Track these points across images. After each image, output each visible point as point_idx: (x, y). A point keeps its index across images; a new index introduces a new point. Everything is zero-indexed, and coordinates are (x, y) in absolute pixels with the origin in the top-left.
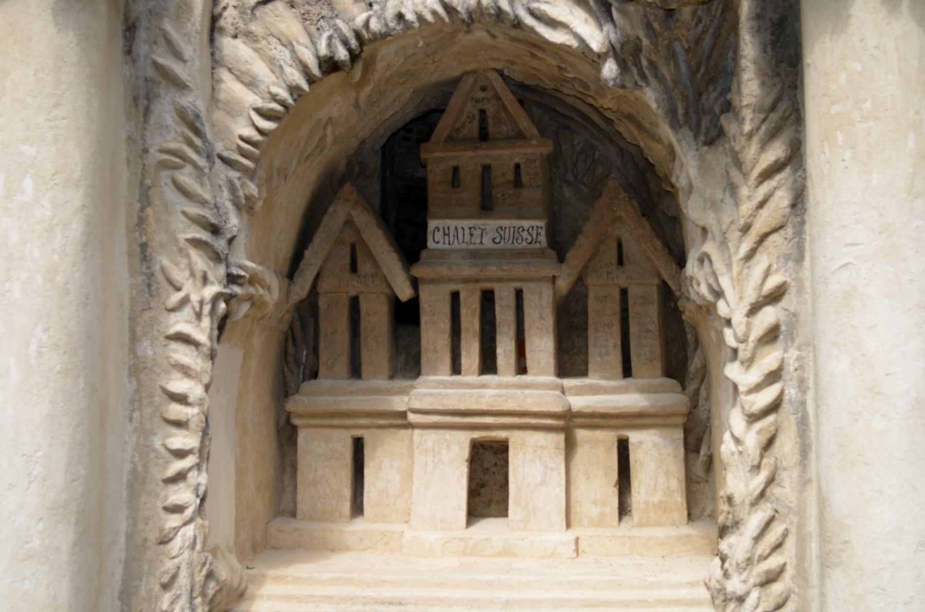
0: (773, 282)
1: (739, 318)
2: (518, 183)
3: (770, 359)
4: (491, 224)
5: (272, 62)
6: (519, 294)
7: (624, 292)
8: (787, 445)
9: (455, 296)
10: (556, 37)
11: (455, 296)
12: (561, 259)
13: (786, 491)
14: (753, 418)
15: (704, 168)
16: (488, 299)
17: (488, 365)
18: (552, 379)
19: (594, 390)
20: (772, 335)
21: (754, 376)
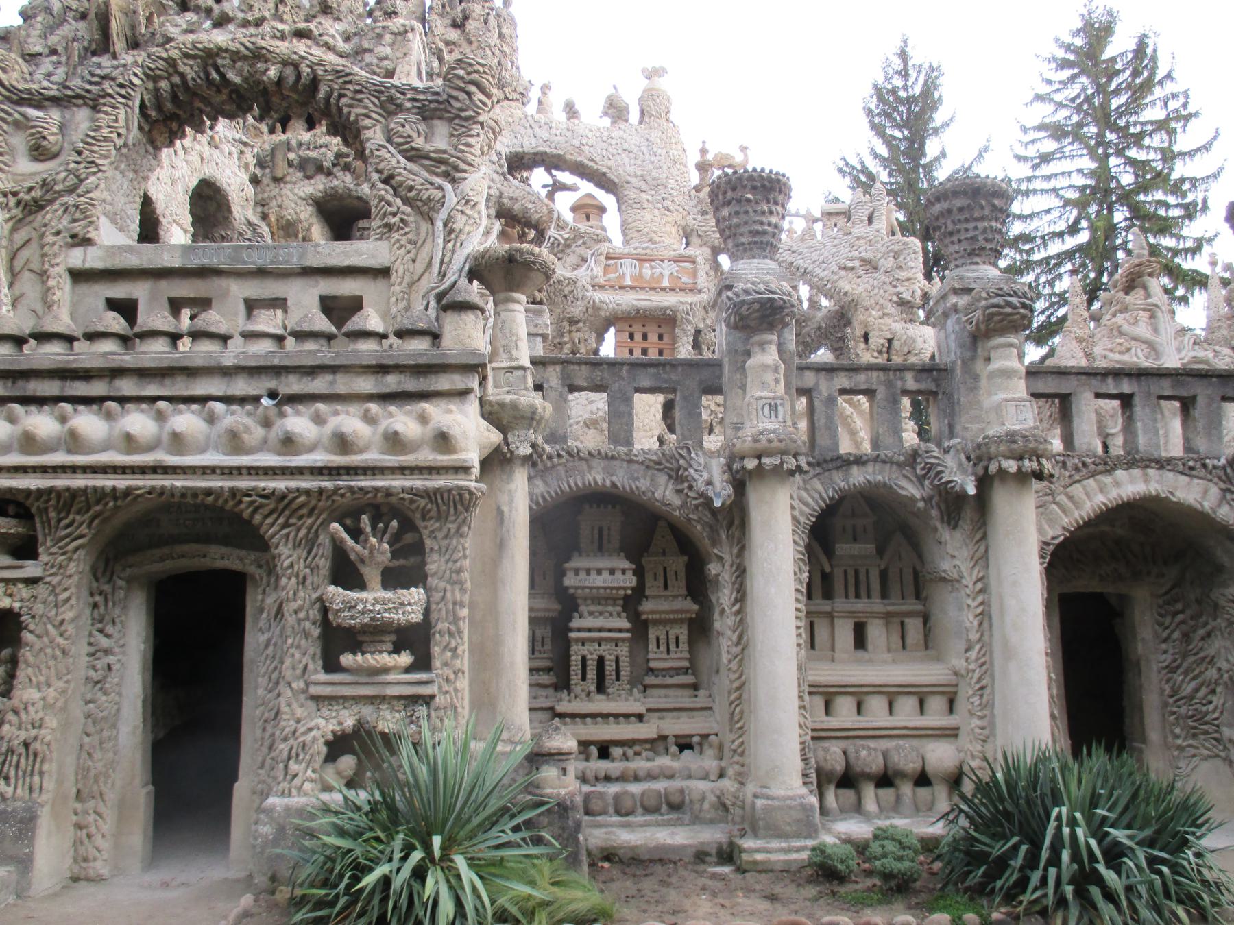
0: (981, 575)
1: (971, 586)
2: (865, 531)
3: (980, 599)
4: (857, 546)
5: (813, 498)
6: (867, 571)
7: (901, 570)
8: (986, 624)
9: (845, 572)
10: (903, 493)
11: (845, 572)
12: (881, 558)
13: (986, 638)
14: (976, 616)
15: (951, 536)
16: (857, 573)
17: (857, 596)
18: (879, 600)
19: (893, 604)
20: (981, 591)
21: (976, 603)
